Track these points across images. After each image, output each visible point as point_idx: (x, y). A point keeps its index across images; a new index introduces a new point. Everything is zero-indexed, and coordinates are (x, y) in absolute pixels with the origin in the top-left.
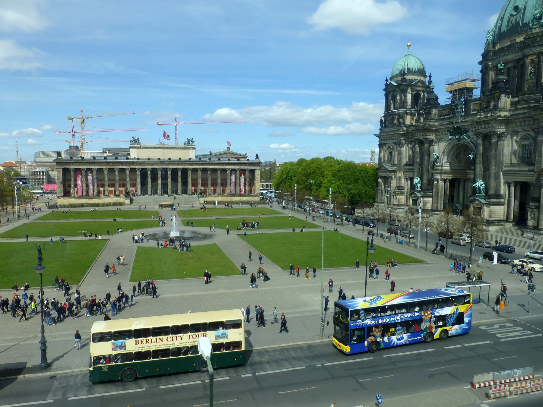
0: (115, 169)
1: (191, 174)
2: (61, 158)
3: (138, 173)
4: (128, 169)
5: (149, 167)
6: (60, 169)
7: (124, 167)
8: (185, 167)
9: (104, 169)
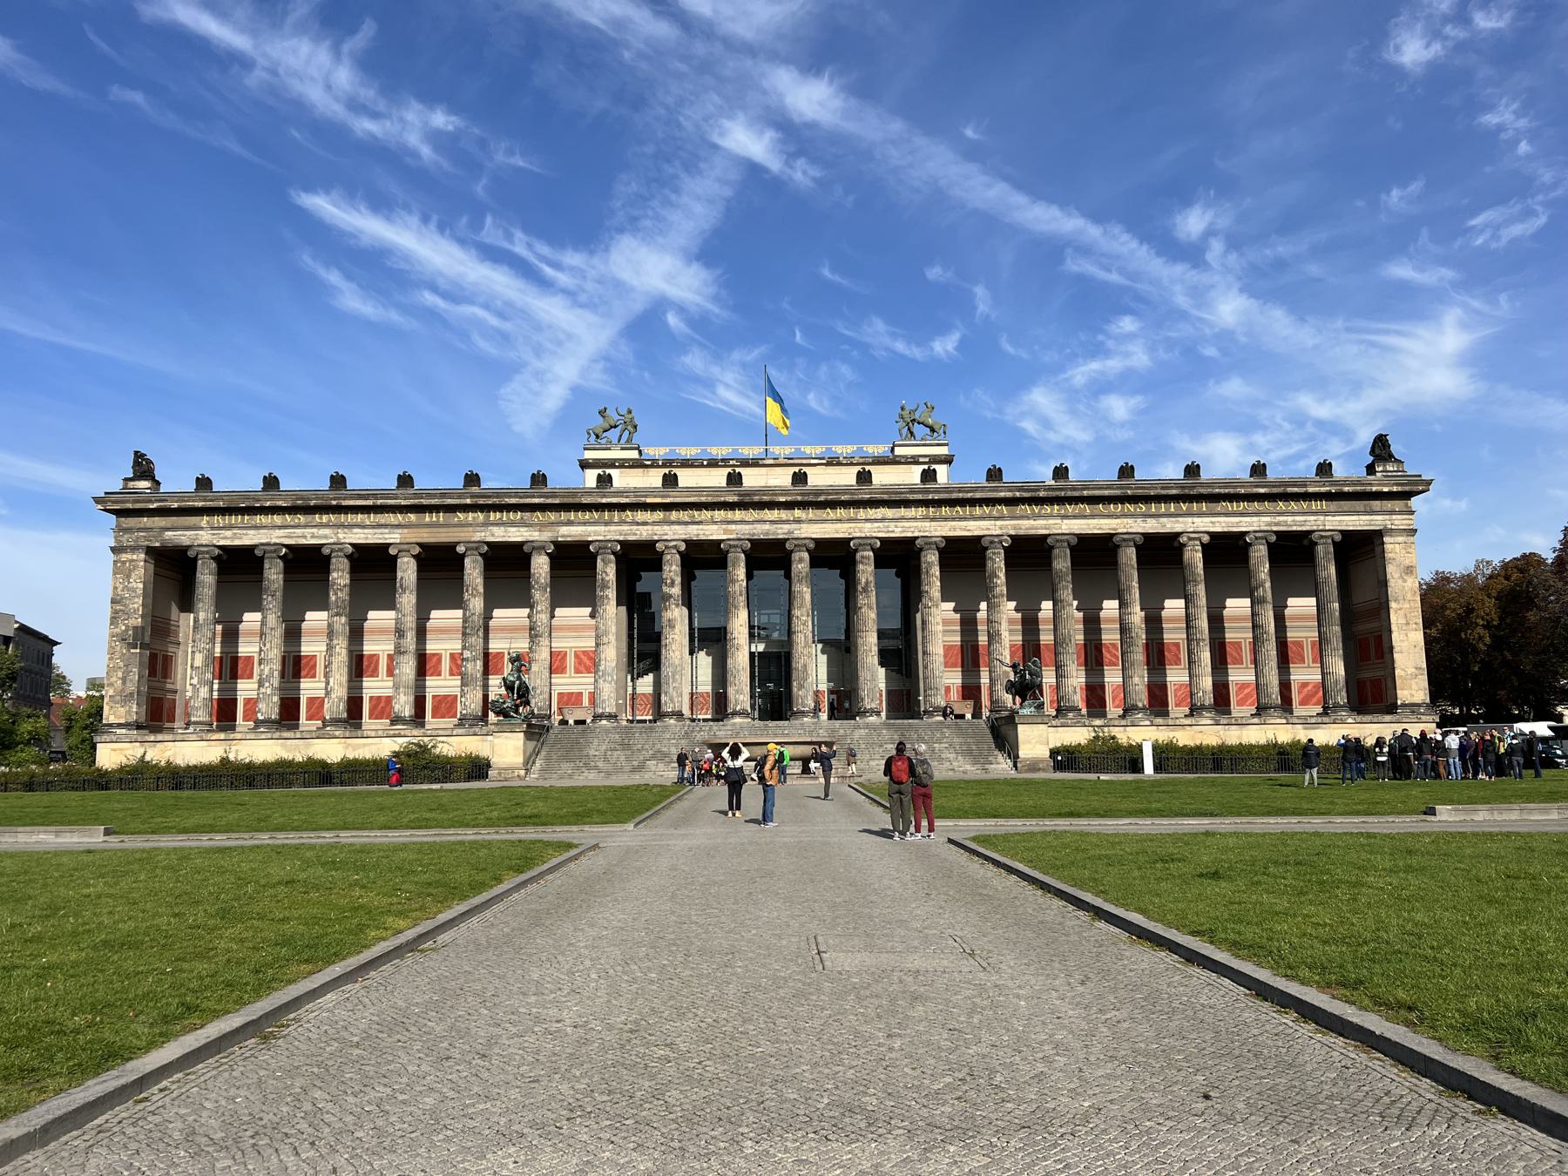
0: (461, 549)
1: (936, 571)
2: (144, 484)
3: (608, 571)
4: (540, 548)
5: (673, 532)
6: (134, 549)
7: (515, 535)
8: (898, 531)
9: (392, 551)
